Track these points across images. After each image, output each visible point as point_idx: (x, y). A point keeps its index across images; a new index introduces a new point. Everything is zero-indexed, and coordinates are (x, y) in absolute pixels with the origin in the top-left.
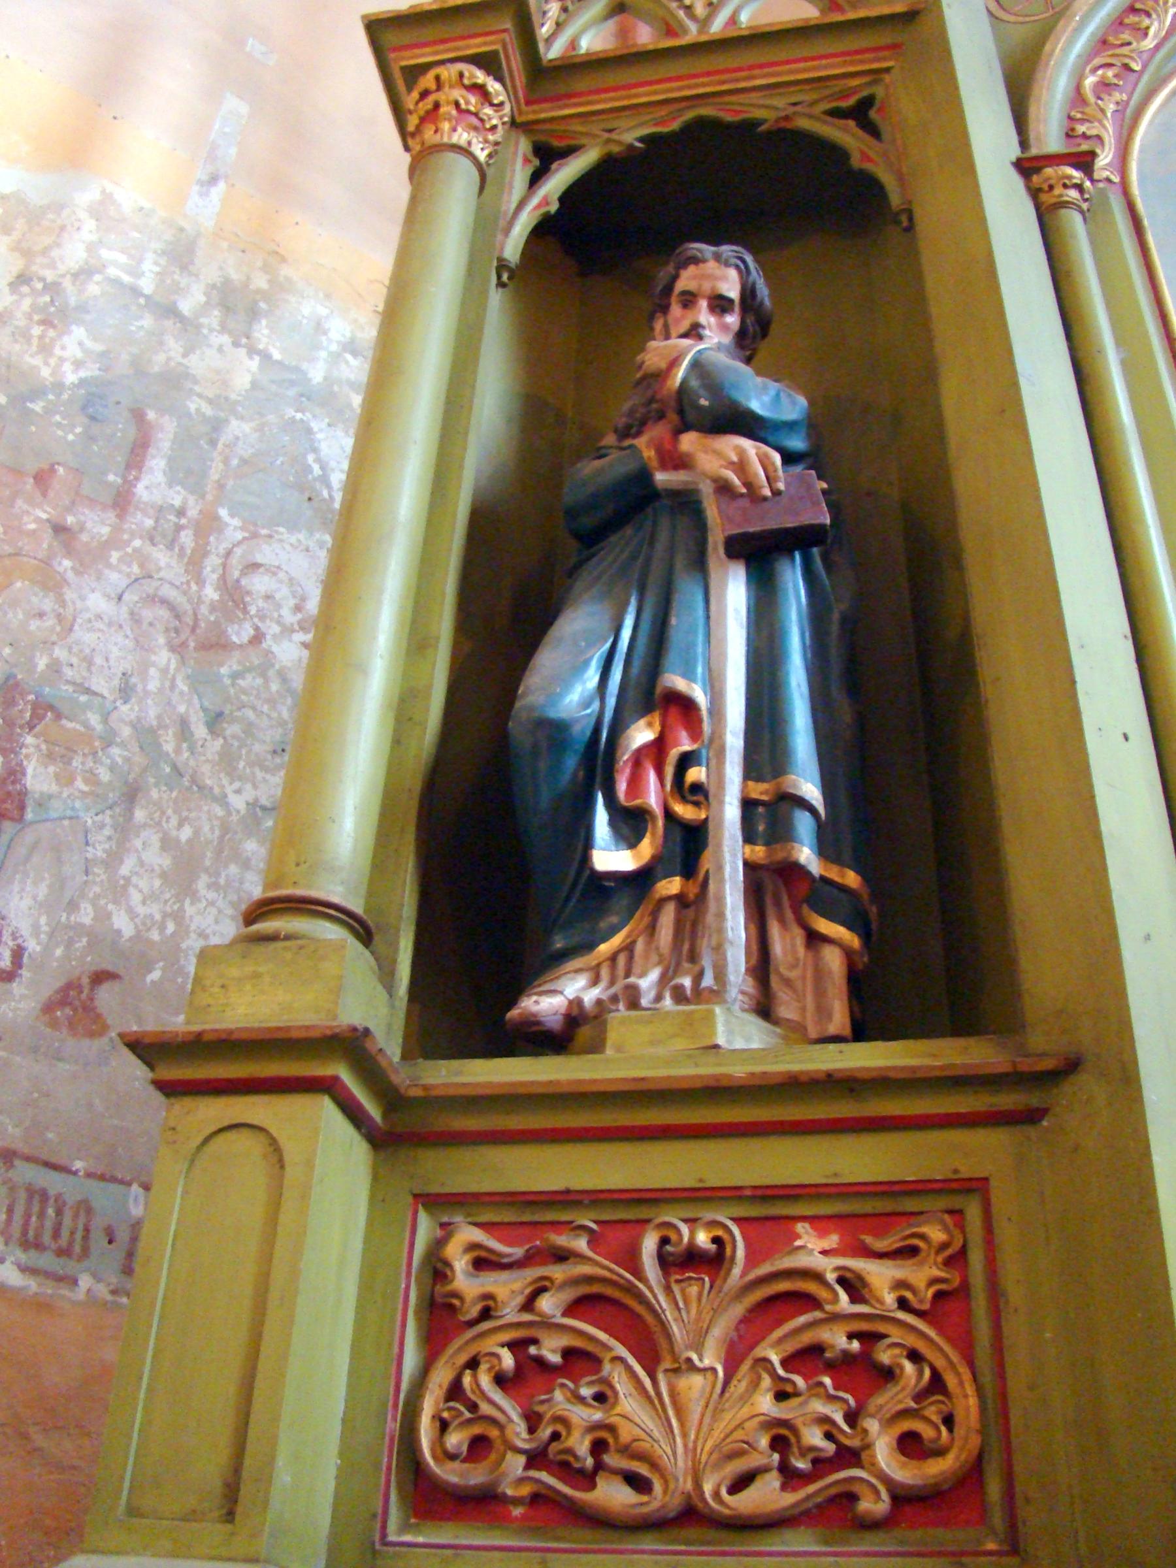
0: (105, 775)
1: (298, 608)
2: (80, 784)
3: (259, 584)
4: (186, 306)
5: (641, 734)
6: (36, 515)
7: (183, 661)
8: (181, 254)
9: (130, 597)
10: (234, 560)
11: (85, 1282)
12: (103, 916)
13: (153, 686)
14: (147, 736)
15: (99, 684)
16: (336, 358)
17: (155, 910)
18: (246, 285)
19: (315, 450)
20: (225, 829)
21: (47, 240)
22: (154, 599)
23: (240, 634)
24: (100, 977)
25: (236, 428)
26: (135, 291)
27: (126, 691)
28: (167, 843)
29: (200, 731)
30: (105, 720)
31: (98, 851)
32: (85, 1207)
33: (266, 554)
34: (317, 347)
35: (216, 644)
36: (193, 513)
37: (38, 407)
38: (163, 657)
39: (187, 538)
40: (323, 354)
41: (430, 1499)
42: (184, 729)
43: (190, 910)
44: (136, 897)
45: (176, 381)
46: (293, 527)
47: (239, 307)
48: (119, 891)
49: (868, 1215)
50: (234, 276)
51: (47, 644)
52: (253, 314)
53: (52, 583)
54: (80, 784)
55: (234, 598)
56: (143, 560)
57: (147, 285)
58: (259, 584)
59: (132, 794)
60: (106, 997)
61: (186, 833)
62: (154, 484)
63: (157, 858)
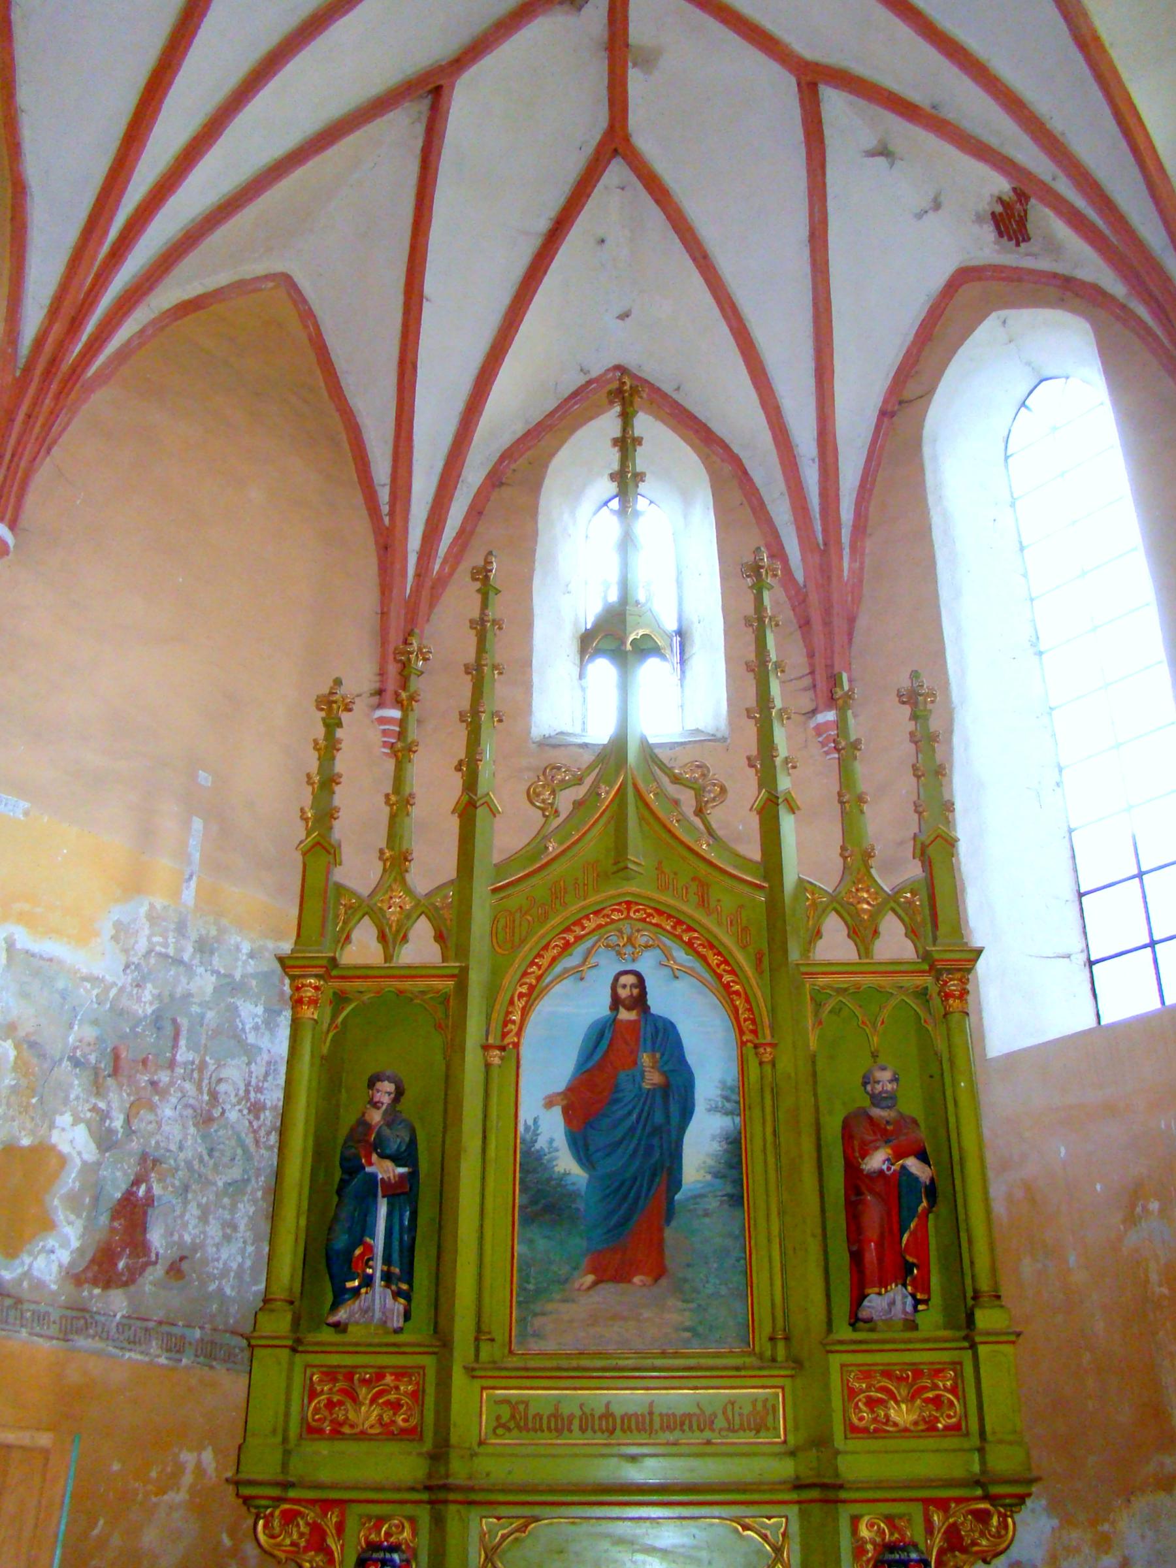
0: (177, 1183)
1: (236, 1095)
2: (170, 1189)
3: (222, 1088)
4: (186, 958)
5: (358, 1252)
6: (144, 1079)
7: (198, 1131)
9: (179, 1107)
10: (213, 1079)
11: (185, 1361)
12: (181, 1237)
13: (190, 1142)
14: (189, 1164)
15: (173, 1147)
16: (245, 962)
17: (196, 1231)
18: (208, 934)
19: (240, 1016)
20: (217, 1194)
21: (133, 940)
22: (186, 1106)
23: (216, 1113)
24: (182, 1259)
26: (167, 956)
27: (181, 1148)
28: (199, 1205)
29: (206, 1158)
30: (175, 1160)
31: (178, 1213)
32: (183, 1337)
33: (225, 1073)
34: (237, 959)
35: (209, 1120)
36: (197, 1062)
37: (139, 1030)
38: (192, 1130)
39: (196, 1075)
40: (240, 963)
42: (201, 1160)
43: (208, 1229)
44: (190, 1227)
46: (233, 1058)
48: (185, 1226)
50: (204, 932)
51: (152, 1134)
52: (212, 953)
53: (152, 1108)
54: (170, 1189)
55: (214, 1095)
56: (181, 1089)
57: (171, 951)
58: (222, 1088)
59: (186, 1188)
60: (185, 1266)
61: (204, 1200)
62: (184, 1054)
63: (196, 1212)
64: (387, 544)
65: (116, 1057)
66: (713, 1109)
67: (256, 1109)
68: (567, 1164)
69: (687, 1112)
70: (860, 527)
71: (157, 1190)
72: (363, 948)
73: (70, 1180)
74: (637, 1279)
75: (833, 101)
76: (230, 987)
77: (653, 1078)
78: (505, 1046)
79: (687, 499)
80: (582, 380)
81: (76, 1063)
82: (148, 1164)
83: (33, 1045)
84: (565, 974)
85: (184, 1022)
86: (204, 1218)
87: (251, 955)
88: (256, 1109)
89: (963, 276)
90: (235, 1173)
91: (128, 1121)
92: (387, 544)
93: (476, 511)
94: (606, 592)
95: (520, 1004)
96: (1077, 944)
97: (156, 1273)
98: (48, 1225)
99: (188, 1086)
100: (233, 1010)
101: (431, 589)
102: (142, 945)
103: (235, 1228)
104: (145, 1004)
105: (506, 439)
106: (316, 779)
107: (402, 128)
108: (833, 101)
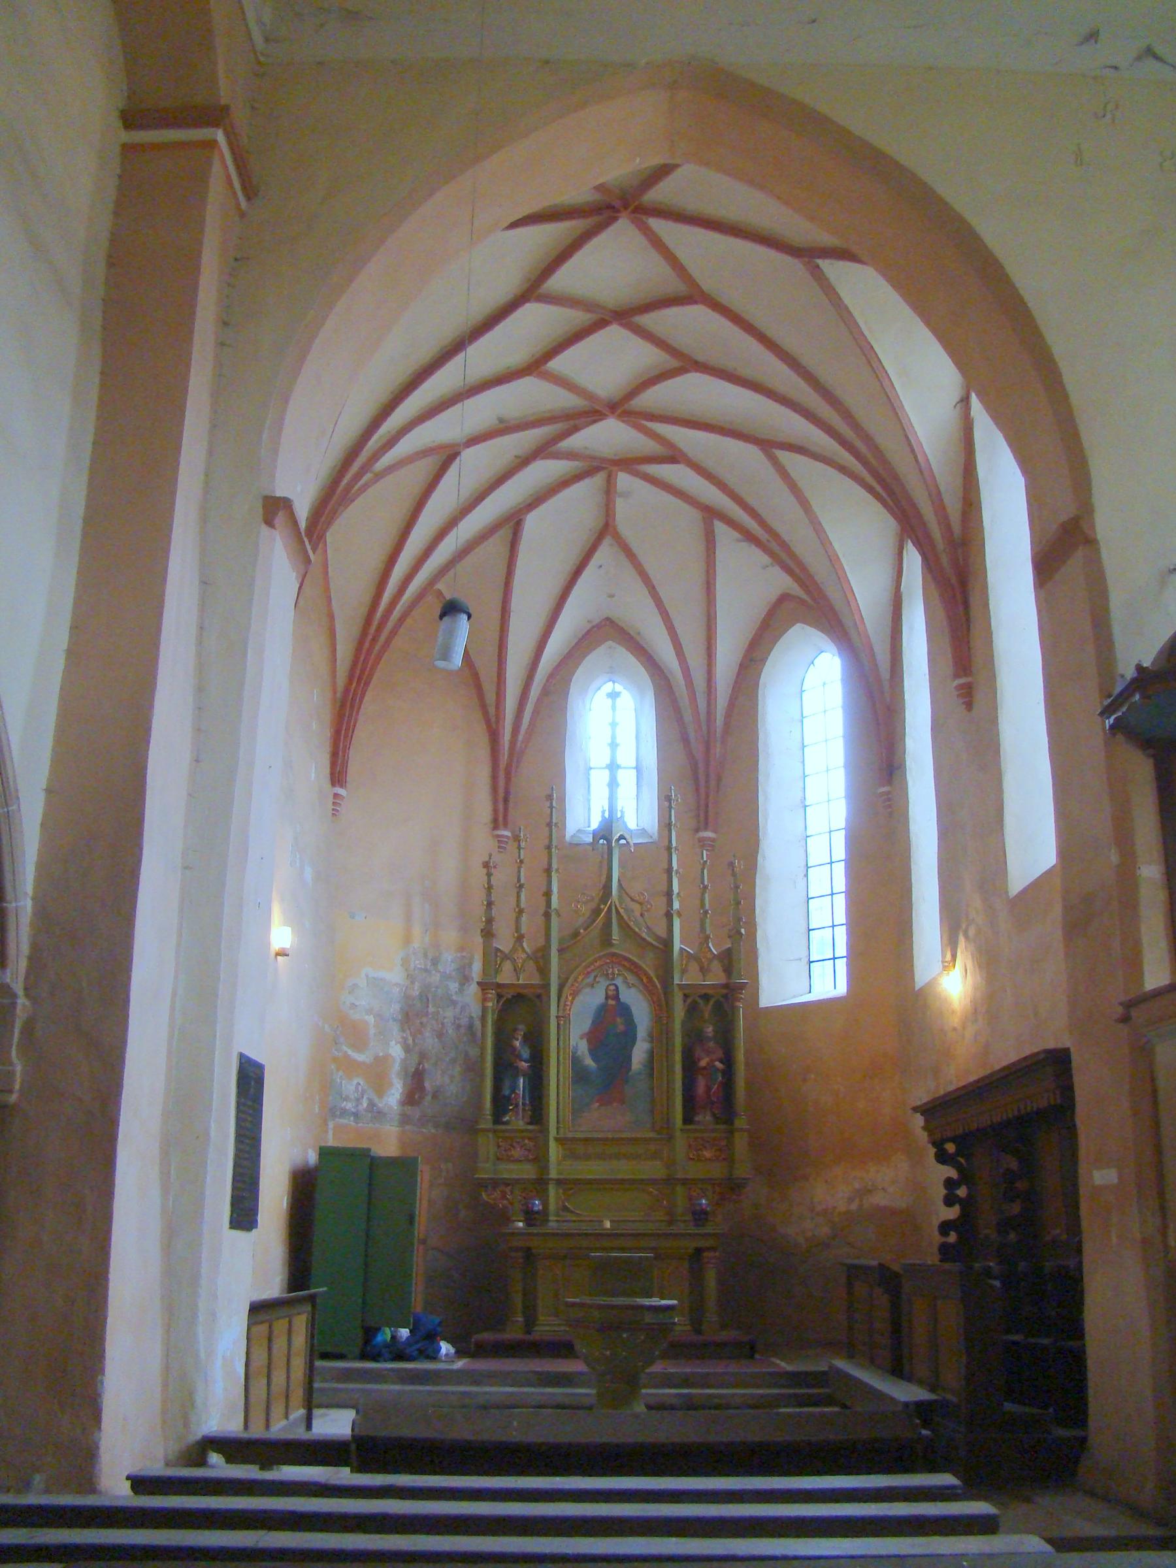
8: (425, 955)
41: (498, 1159)
47: (435, 962)
49: (530, 1139)
55: (443, 1024)
62: (431, 1009)
64: (494, 736)
65: (407, 1014)
67: (459, 1027)
68: (589, 1062)
71: (426, 1066)
72: (506, 976)
73: (397, 1067)
74: (615, 1104)
75: (720, 527)
77: (621, 1028)
78: (563, 1019)
80: (589, 626)
81: (394, 1020)
82: (423, 1056)
88: (459, 1027)
89: (784, 598)
90: (453, 1054)
92: (494, 736)
93: (536, 712)
96: (804, 953)
97: (429, 1098)
98: (391, 1085)
101: (515, 753)
102: (412, 965)
104: (416, 992)
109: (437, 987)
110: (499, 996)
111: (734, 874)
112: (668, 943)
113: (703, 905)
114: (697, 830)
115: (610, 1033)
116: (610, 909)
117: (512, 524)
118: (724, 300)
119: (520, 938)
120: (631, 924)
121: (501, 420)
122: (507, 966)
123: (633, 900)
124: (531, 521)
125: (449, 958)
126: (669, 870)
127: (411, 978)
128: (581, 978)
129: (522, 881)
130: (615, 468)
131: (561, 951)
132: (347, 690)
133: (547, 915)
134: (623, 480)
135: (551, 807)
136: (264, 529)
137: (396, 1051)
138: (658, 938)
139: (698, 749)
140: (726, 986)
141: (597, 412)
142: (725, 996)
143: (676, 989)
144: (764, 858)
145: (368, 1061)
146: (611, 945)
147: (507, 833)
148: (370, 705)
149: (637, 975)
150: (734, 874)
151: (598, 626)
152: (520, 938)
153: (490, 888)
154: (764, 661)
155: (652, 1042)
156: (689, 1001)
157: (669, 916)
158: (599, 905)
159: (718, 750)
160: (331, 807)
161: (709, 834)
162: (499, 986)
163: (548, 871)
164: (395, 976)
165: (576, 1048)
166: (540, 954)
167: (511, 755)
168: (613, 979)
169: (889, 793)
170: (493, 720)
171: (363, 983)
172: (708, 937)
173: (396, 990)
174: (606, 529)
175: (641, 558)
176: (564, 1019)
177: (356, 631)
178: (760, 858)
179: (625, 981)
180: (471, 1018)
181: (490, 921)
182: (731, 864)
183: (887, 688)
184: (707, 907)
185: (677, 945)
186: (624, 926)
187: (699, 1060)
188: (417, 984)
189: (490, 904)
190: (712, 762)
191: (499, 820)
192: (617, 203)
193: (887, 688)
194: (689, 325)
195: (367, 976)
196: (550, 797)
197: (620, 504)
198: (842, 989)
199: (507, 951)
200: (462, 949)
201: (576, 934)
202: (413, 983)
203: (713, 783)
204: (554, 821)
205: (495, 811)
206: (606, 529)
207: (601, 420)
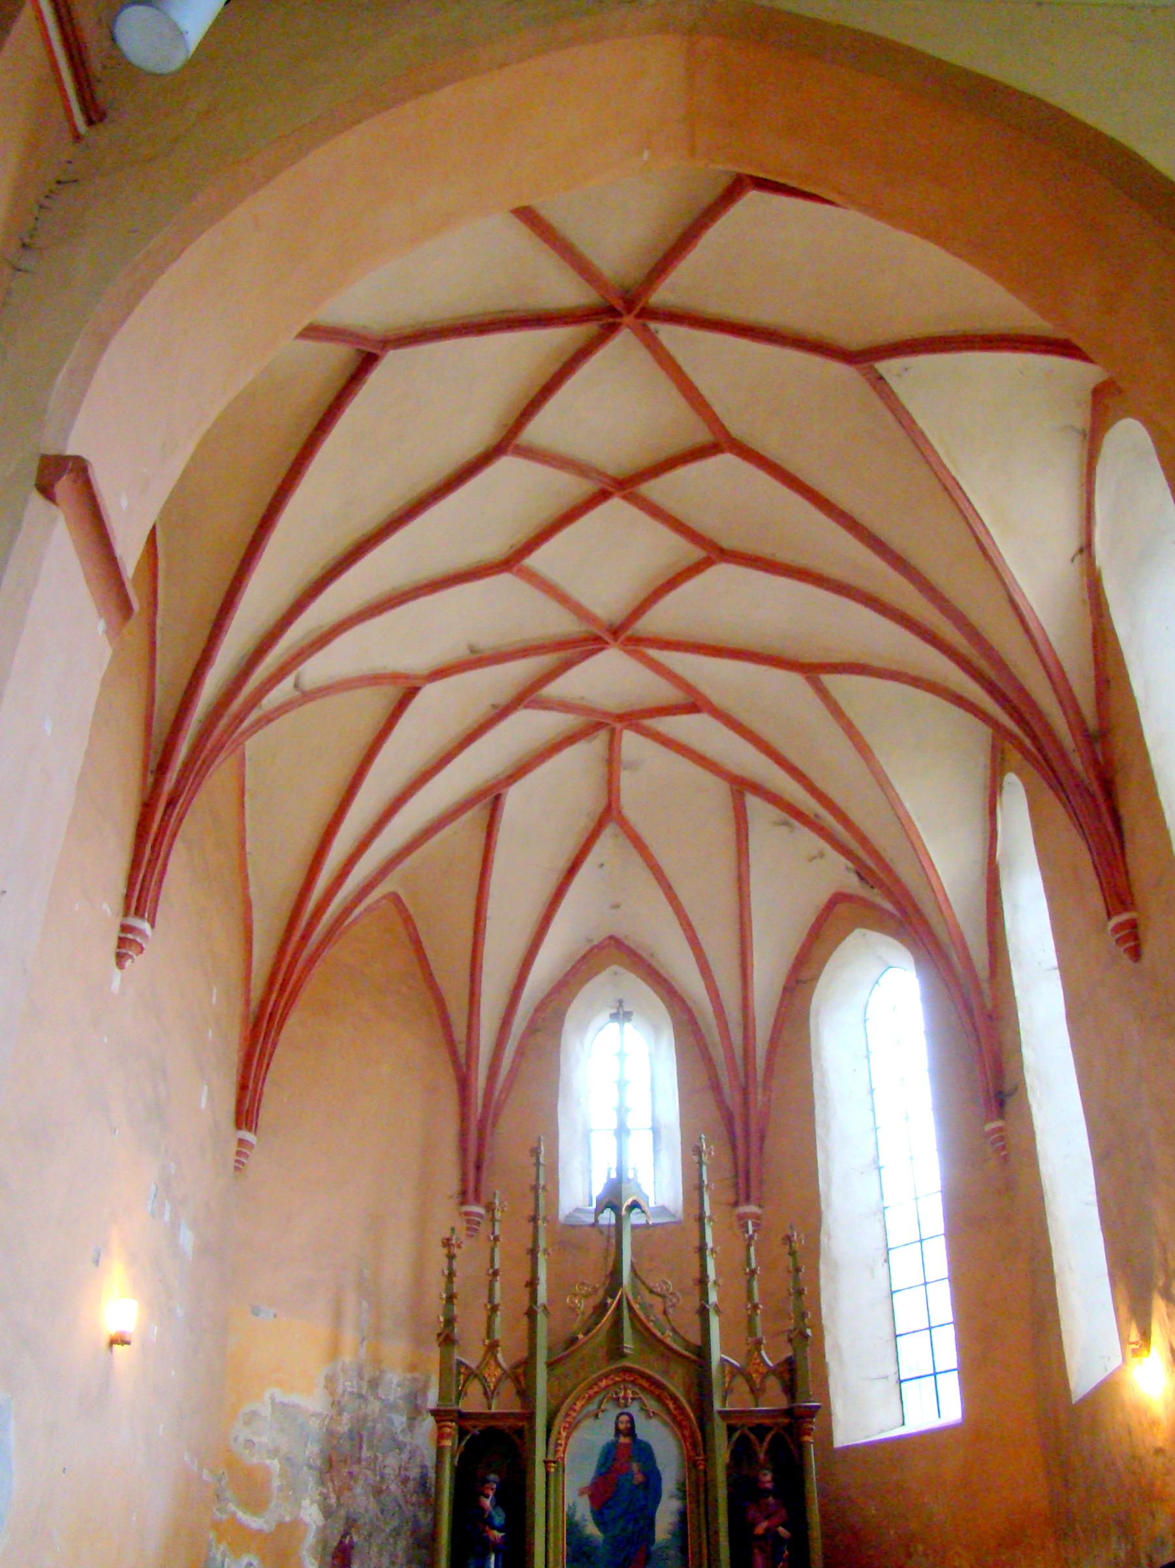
3: (387, 1471)
4: (364, 1392)
8: (361, 1377)
25: (379, 1426)
27: (367, 1511)
38: (372, 1499)
45: (364, 1419)
47: (374, 1384)
55: (382, 1476)
57: (355, 1390)
58: (387, 1471)
62: (366, 1453)
64: (464, 1084)
65: (330, 1460)
66: (671, 1496)
67: (405, 1480)
68: (592, 1529)
69: (657, 1501)
70: (769, 1068)
71: (356, 1538)
72: (473, 1401)
73: (311, 1539)
75: (753, 802)
76: (390, 1407)
79: (656, 1029)
80: (588, 947)
81: (310, 1467)
82: (351, 1523)
83: (289, 1459)
84: (587, 1416)
85: (365, 1434)
86: (380, 1553)
87: (398, 1385)
89: (838, 899)
90: (395, 1523)
91: (338, 1498)
92: (464, 1084)
93: (520, 1053)
94: (609, 1174)
95: (564, 1434)
96: (892, 1369)
99: (369, 1473)
100: (390, 1421)
102: (340, 1390)
103: (396, 1556)
104: (344, 1427)
105: (540, 996)
106: (444, 1296)
107: (475, 816)
108: (753, 802)
109: (375, 1421)
110: (462, 1432)
111: (792, 1253)
112: (702, 1353)
113: (750, 1297)
114: (736, 1204)
115: (623, 1483)
116: (620, 1303)
117: (490, 799)
118: (757, 445)
119: (493, 1347)
120: (651, 1325)
121: (472, 650)
122: (475, 1388)
123: (651, 1292)
124: (513, 797)
125: (395, 1382)
126: (702, 1249)
127: (337, 1406)
128: (579, 1404)
129: (497, 1266)
130: (618, 726)
131: (551, 1365)
132: (263, 1003)
133: (531, 1314)
134: (630, 741)
135: (538, 1164)
136: (37, 499)
137: (311, 1514)
138: (688, 1345)
139: (732, 1098)
140: (788, 1413)
141: (597, 639)
142: (788, 1428)
143: (717, 1419)
144: (829, 1237)
145: (266, 1528)
146: (623, 1356)
147: (480, 1210)
148: (296, 1026)
149: (659, 1399)
150: (792, 1253)
151: (600, 947)
152: (493, 1347)
153: (451, 1275)
154: (815, 978)
155: (683, 1498)
156: (737, 1435)
157: (703, 1312)
158: (605, 1299)
159: (759, 1097)
160: (233, 1156)
161: (752, 1209)
162: (462, 1416)
163: (533, 1252)
164: (313, 1402)
165: (573, 1508)
166: (520, 1371)
167: (486, 1106)
168: (626, 1406)
169: (1000, 1129)
170: (463, 1060)
171: (267, 1411)
172: (758, 1343)
173: (314, 1424)
174: (610, 812)
175: (654, 849)
176: (554, 1464)
177: (280, 924)
178: (823, 1238)
179: (643, 1409)
180: (424, 1467)
181: (450, 1321)
182: (788, 1239)
183: (985, 986)
184: (756, 1298)
185: (716, 1354)
186: (644, 1333)
187: (754, 1525)
188: (346, 1417)
189: (451, 1298)
190: (752, 1112)
191: (470, 1190)
192: (619, 305)
193: (985, 986)
194: (714, 491)
195: (273, 1399)
196: (535, 1152)
197: (626, 781)
198: (953, 1413)
199: (473, 1366)
200: (413, 1367)
201: (573, 1340)
202: (340, 1413)
203: (754, 1139)
204: (542, 1182)
205: (464, 1180)
206: (610, 812)
207: (601, 649)
